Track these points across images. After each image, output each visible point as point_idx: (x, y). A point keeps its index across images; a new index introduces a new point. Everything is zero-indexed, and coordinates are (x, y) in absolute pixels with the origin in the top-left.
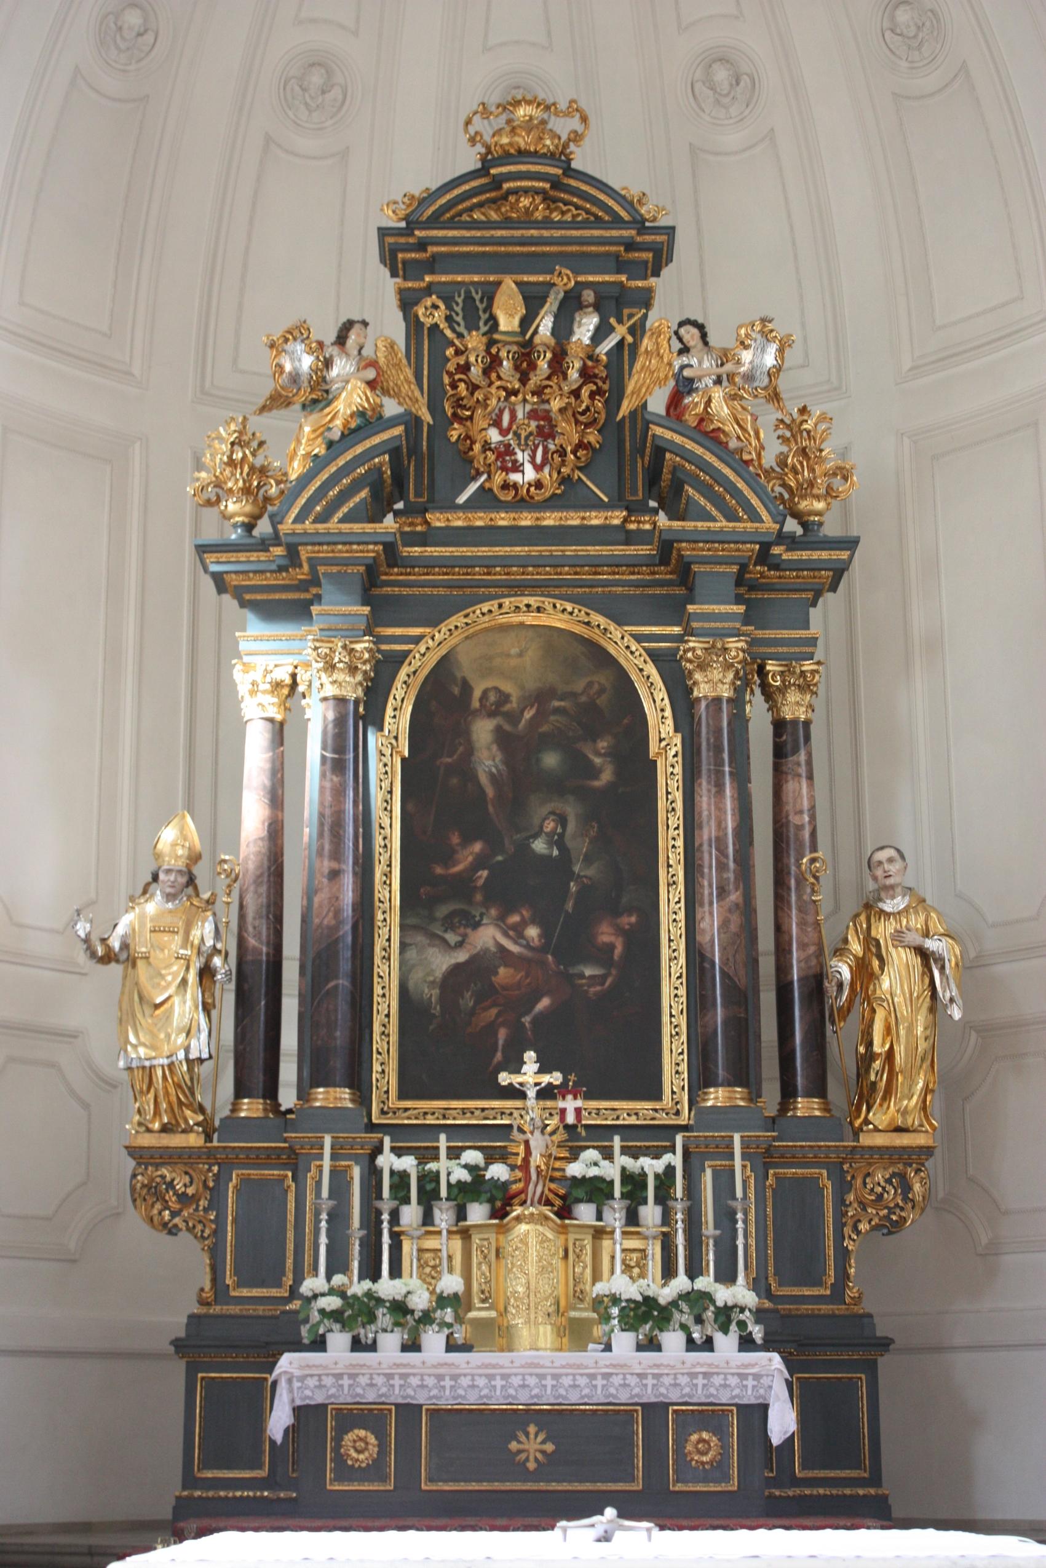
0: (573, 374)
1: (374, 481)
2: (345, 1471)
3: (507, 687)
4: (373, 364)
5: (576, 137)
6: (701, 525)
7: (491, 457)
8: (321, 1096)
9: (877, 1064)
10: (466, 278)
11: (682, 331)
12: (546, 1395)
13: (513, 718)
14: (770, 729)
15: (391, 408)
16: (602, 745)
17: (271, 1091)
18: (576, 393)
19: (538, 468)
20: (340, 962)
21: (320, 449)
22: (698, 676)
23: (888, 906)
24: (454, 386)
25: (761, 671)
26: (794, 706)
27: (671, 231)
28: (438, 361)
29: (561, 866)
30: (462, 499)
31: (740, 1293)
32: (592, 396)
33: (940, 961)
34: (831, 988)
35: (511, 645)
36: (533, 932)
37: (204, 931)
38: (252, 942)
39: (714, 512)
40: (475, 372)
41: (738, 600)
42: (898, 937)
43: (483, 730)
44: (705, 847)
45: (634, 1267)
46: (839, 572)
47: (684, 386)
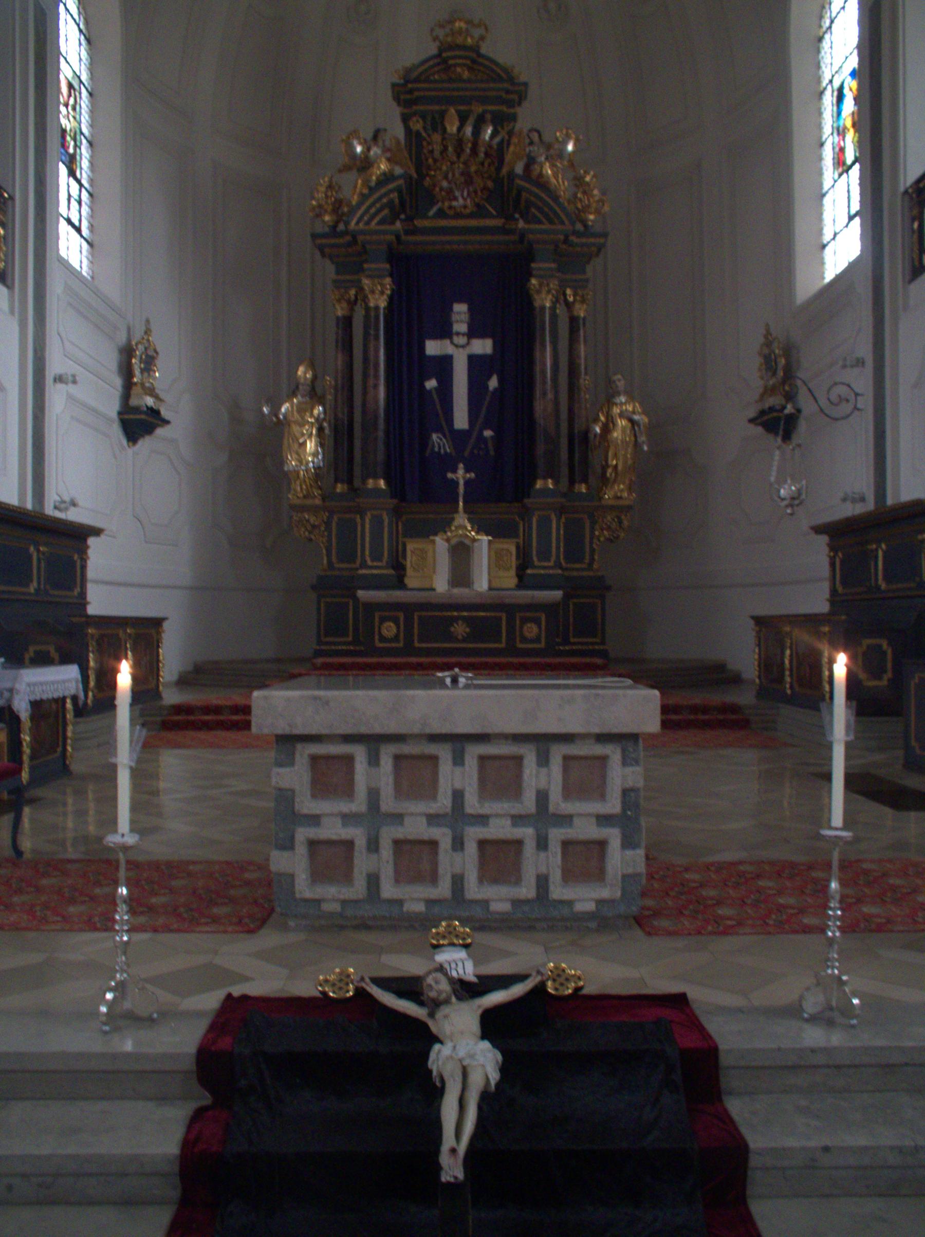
0: (482, 155)
1: (390, 204)
2: (383, 639)
4: (389, 150)
5: (482, 38)
6: (537, 226)
7: (443, 193)
8: (371, 483)
9: (609, 470)
10: (431, 108)
11: (531, 135)
14: (567, 320)
15: (398, 171)
17: (350, 481)
18: (482, 164)
19: (465, 199)
21: (365, 191)
22: (536, 297)
23: (617, 400)
24: (427, 160)
25: (565, 294)
27: (525, 84)
30: (431, 213)
32: (489, 165)
33: (639, 426)
34: (591, 436)
37: (319, 410)
38: (340, 415)
39: (544, 220)
40: (437, 154)
41: (554, 261)
42: (621, 415)
44: (538, 373)
46: (600, 248)
47: (531, 161)
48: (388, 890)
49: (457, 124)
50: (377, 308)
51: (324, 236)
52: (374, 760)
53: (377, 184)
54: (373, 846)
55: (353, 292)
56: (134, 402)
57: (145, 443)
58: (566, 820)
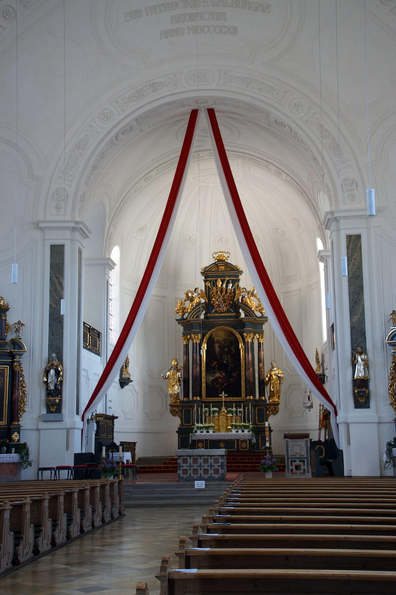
3: (220, 339)
4: (199, 294)
12: (223, 438)
13: (221, 343)
16: (233, 347)
17: (188, 397)
20: (197, 379)
28: (209, 291)
34: (265, 381)
35: (220, 333)
36: (224, 374)
40: (215, 293)
43: (217, 345)
46: (267, 321)
47: (243, 297)
48: (192, 475)
49: (221, 283)
50: (196, 343)
51: (180, 320)
52: (190, 459)
53: (196, 306)
54: (190, 470)
55: (189, 336)
56: (123, 376)
57: (126, 387)
58: (214, 466)
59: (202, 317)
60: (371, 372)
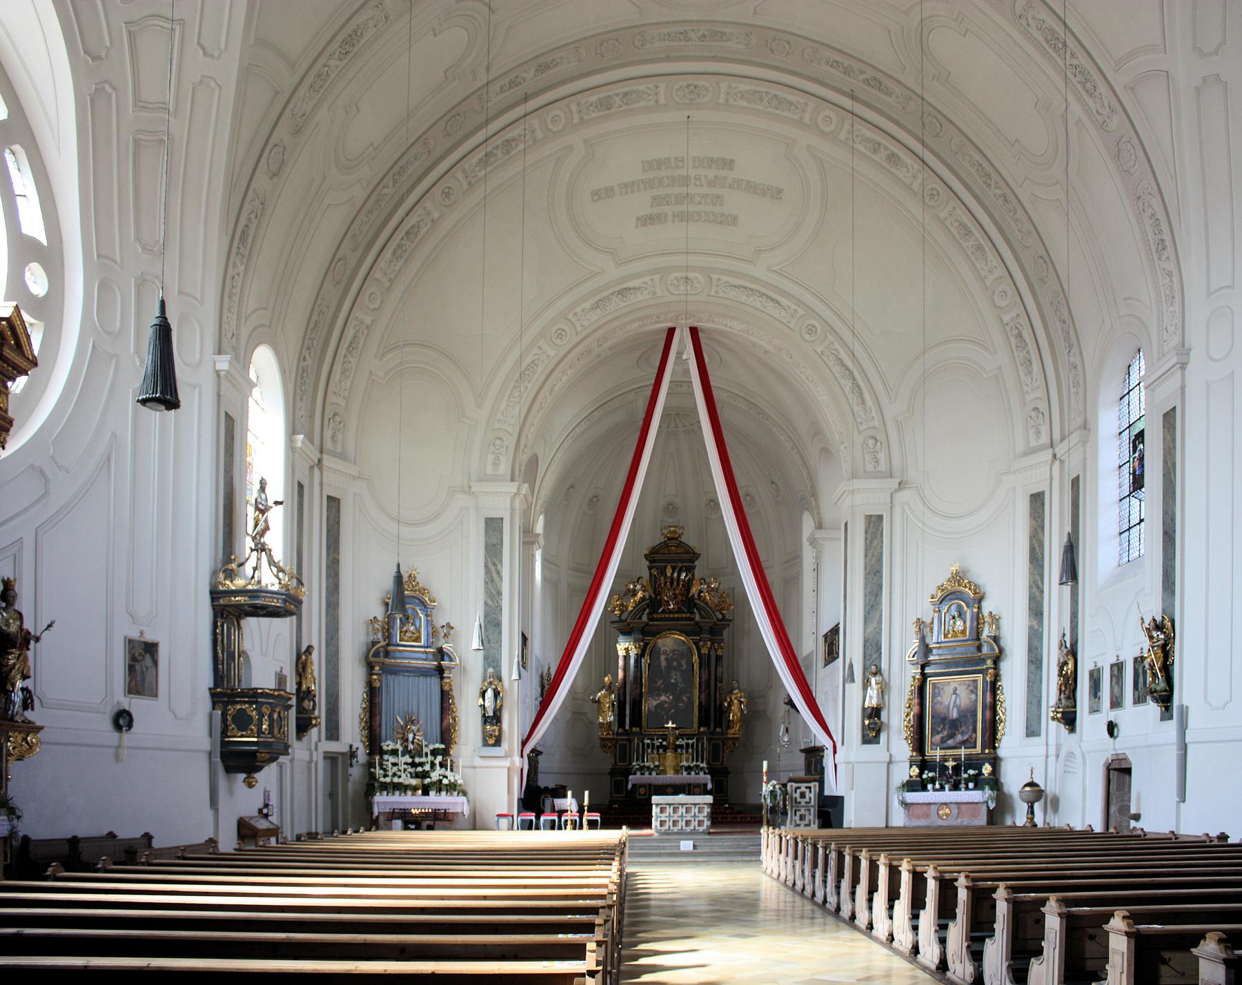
26: (720, 653)
29: (676, 685)
31: (704, 765)
43: (663, 658)
45: (687, 760)
47: (701, 592)
59: (645, 618)
60: (886, 698)
